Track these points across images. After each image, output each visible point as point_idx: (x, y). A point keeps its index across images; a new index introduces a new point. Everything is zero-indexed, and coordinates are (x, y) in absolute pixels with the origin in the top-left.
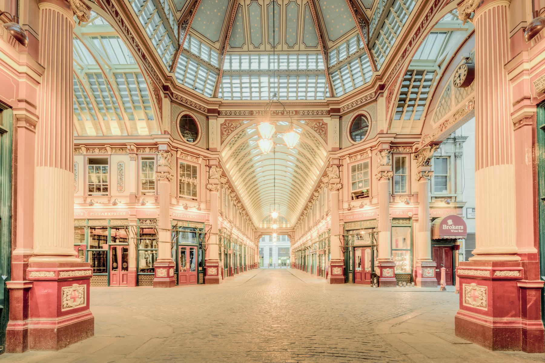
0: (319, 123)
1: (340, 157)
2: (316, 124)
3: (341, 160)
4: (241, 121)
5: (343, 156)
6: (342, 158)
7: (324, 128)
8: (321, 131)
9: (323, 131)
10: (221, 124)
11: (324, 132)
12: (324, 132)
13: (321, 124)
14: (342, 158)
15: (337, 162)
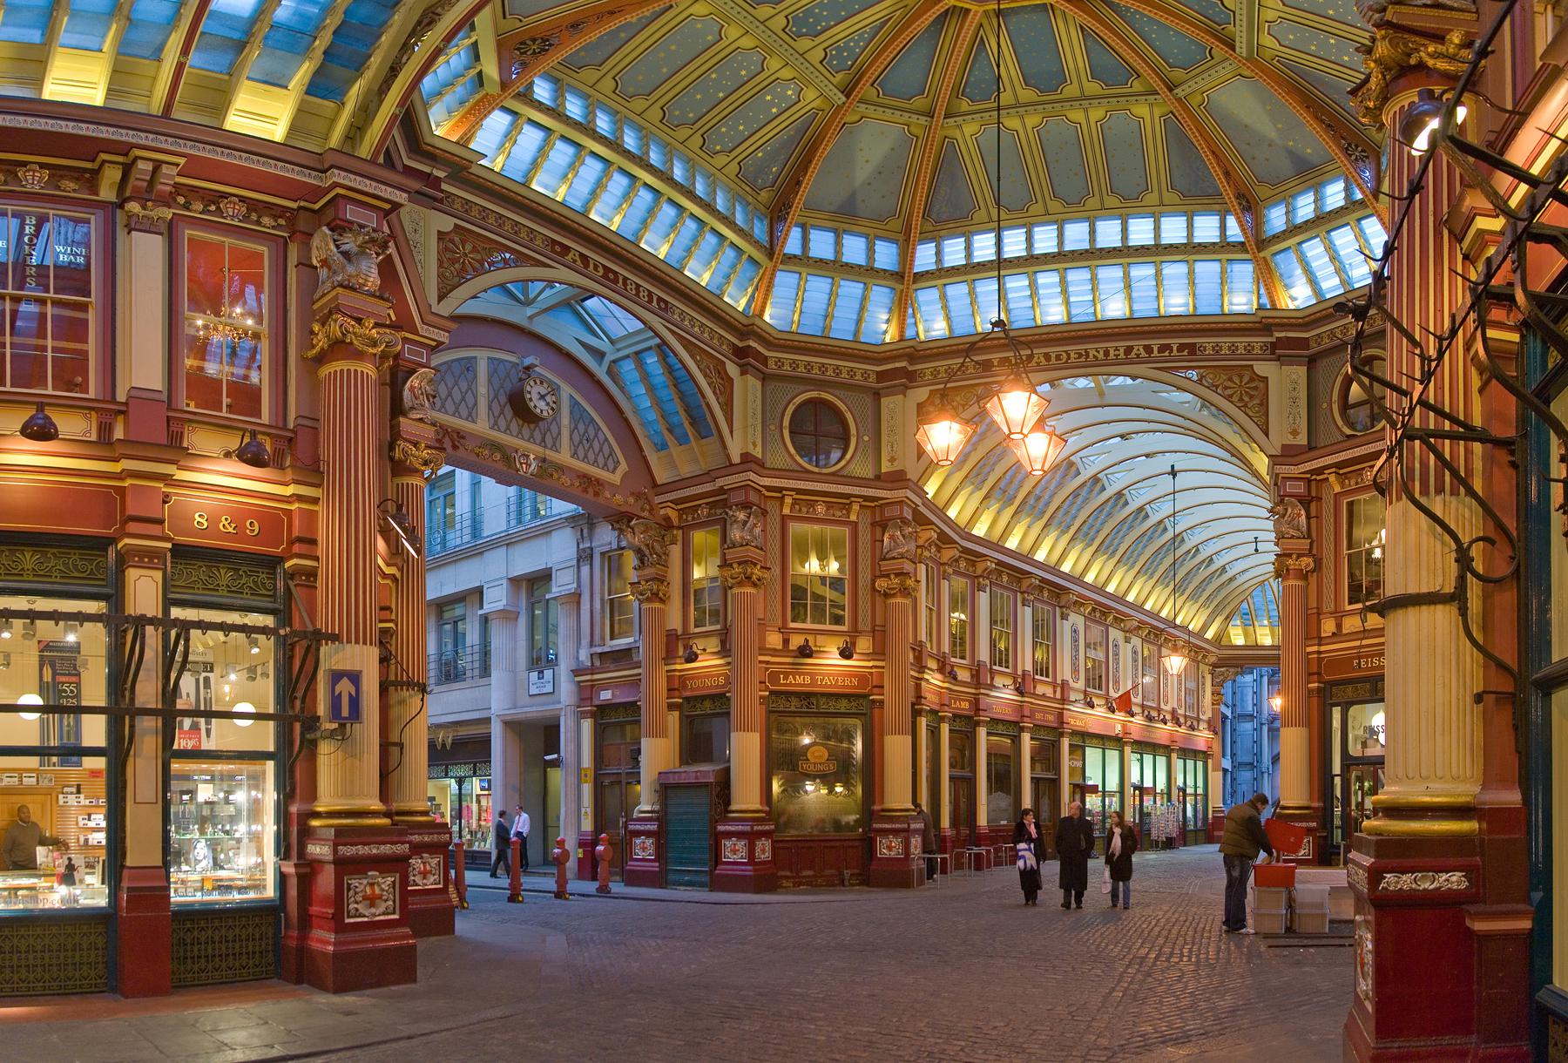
0: (1241, 377)
1: (1312, 472)
2: (1230, 379)
3: (1313, 483)
4: (980, 390)
5: (1320, 471)
6: (1318, 478)
7: (1256, 388)
8: (1246, 399)
9: (1251, 397)
10: (918, 404)
11: (1256, 401)
12: (1256, 401)
13: (1246, 379)
14: (1318, 478)
15: (1300, 488)
